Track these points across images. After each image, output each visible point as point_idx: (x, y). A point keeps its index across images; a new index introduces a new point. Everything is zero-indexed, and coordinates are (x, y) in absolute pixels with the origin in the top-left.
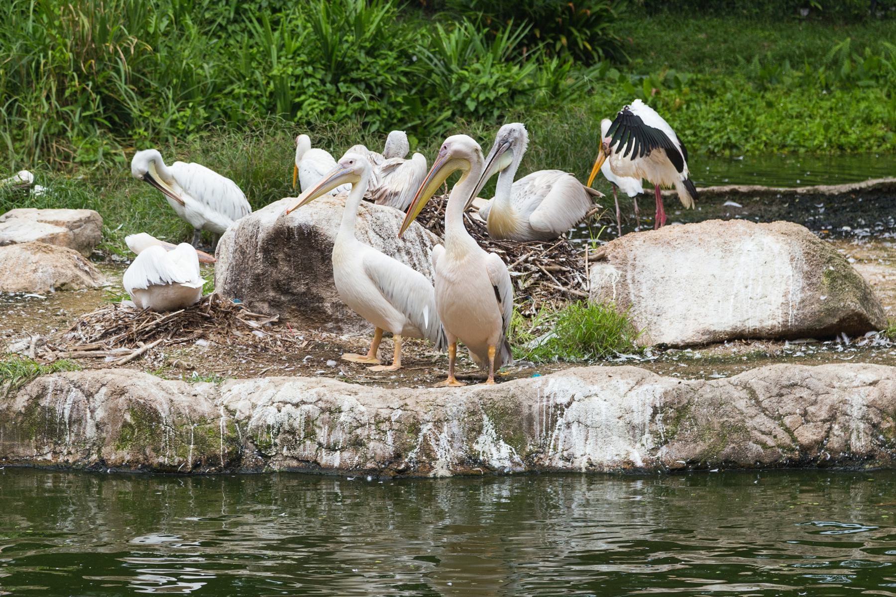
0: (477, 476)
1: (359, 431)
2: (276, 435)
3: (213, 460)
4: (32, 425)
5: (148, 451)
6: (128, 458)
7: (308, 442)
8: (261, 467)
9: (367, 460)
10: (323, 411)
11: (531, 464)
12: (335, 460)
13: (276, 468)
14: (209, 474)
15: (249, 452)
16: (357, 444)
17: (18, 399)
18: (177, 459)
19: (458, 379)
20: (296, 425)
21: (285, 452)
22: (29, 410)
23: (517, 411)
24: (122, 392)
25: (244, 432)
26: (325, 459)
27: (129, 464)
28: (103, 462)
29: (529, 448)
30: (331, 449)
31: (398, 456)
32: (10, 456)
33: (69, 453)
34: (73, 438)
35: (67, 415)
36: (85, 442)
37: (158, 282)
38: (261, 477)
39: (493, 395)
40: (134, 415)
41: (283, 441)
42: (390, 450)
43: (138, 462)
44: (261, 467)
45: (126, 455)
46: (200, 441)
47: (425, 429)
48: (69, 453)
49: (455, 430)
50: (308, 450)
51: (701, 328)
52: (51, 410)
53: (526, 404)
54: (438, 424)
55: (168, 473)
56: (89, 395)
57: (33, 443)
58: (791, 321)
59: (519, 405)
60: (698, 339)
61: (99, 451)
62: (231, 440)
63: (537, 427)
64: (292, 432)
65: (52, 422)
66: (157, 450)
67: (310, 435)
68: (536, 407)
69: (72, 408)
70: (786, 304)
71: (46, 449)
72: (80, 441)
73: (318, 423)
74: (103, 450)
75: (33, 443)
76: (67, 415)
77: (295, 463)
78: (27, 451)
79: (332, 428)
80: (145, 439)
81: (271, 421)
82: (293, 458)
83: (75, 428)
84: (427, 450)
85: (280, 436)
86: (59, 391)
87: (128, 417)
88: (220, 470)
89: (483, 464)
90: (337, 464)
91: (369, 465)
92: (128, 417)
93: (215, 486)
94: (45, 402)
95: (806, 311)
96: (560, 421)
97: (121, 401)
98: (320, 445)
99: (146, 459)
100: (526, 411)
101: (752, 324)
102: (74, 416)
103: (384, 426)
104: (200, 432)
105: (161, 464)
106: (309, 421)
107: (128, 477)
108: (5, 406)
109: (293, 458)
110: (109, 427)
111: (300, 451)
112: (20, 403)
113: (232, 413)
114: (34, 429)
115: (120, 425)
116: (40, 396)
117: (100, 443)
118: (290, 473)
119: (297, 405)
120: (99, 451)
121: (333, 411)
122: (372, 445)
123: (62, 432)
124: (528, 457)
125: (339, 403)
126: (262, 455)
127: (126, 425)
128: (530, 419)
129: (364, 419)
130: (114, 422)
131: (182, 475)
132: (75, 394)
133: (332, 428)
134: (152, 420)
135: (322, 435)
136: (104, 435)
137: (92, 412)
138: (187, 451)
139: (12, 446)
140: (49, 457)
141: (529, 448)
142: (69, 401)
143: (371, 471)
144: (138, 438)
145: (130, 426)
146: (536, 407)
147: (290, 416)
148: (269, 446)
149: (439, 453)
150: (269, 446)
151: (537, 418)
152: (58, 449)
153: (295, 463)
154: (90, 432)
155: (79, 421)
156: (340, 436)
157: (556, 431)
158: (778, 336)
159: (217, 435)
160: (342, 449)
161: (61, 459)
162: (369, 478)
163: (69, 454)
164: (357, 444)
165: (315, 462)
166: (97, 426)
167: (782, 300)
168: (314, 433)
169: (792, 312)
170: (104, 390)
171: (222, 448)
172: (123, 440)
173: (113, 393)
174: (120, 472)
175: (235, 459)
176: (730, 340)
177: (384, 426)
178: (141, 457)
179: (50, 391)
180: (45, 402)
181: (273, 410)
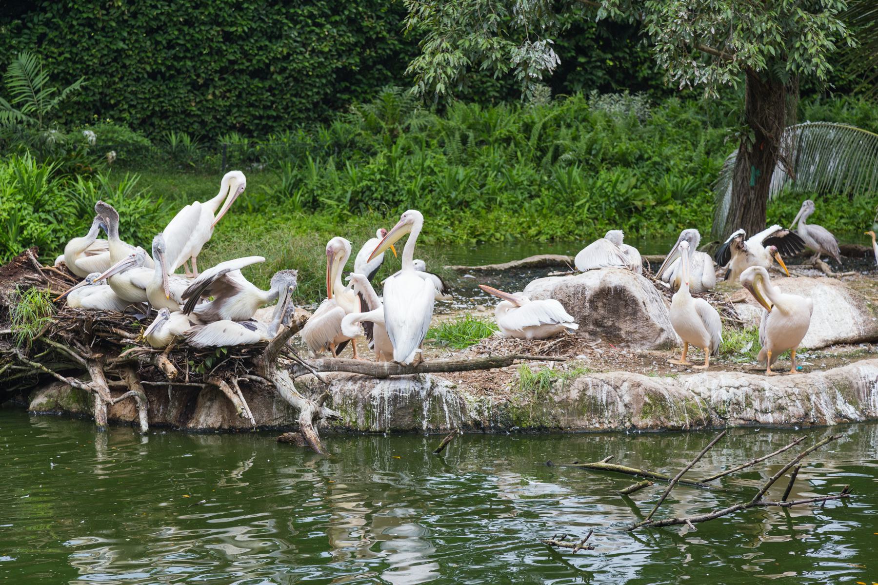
0: (845, 423)
1: (780, 401)
2: (728, 406)
3: (699, 422)
4: (583, 407)
5: (662, 418)
6: (650, 423)
7: (748, 409)
8: (724, 425)
9: (790, 417)
10: (754, 391)
11: (867, 417)
12: (770, 418)
13: (733, 425)
14: (699, 430)
15: (714, 416)
16: (781, 408)
17: (572, 392)
18: (681, 423)
19: (799, 371)
20: (740, 399)
21: (735, 415)
22: (581, 399)
23: (851, 387)
24: (639, 385)
25: (709, 405)
26: (762, 418)
27: (652, 427)
28: (634, 427)
29: (861, 407)
30: (765, 412)
31: (807, 415)
32: (572, 426)
33: (610, 422)
34: (610, 413)
35: (604, 400)
36: (619, 415)
37: (549, 321)
38: (724, 429)
39: (836, 378)
40: (650, 397)
41: (733, 409)
42: (802, 412)
43: (657, 425)
44: (724, 425)
45: (649, 421)
46: (690, 412)
47: (813, 398)
48: (610, 422)
49: (826, 398)
50: (749, 414)
51: (821, 338)
52: (594, 398)
53: (854, 381)
54: (817, 394)
55: (677, 431)
56: (616, 388)
57: (585, 418)
58: (863, 334)
59: (851, 383)
60: (822, 345)
61: (630, 420)
62: (705, 410)
63: (862, 395)
64: (738, 403)
65: (595, 404)
66: (668, 418)
67: (749, 405)
68: (860, 383)
69: (607, 396)
70: (856, 323)
71: (594, 421)
72: (615, 415)
73: (753, 397)
74: (632, 419)
75: (585, 418)
76: (604, 400)
77: (742, 422)
78: (582, 423)
79: (762, 400)
80: (659, 411)
81: (725, 398)
82: (741, 419)
83: (611, 407)
84: (818, 411)
85: (731, 406)
86: (596, 386)
87: (647, 399)
88: (705, 428)
89: (845, 417)
90: (771, 420)
91: (793, 420)
92: (647, 399)
93: (701, 437)
94: (590, 392)
95: (869, 326)
96: (873, 391)
97: (640, 389)
98: (756, 410)
99: (662, 423)
100: (856, 386)
101: (843, 336)
102: (610, 400)
103: (793, 397)
104: (689, 406)
105: (673, 426)
106: (747, 397)
107: (652, 435)
108: (565, 396)
109: (741, 419)
110: (635, 406)
111: (744, 415)
112: (574, 394)
113: (699, 394)
114: (585, 409)
115: (642, 404)
116: (584, 390)
117: (630, 416)
118: (742, 427)
119: (738, 388)
120: (630, 420)
121: (760, 390)
122: (790, 408)
123: (602, 410)
124: (862, 412)
125: (762, 386)
126: (723, 419)
127: (646, 404)
128: (858, 390)
129: (781, 394)
130: (638, 402)
131: (685, 431)
132: (606, 388)
133: (762, 400)
134: (662, 400)
135: (756, 404)
136: (631, 411)
137: (620, 397)
138: (685, 418)
139: (573, 420)
140: (597, 425)
141: (861, 407)
142: (604, 392)
143: (796, 424)
144: (655, 412)
145: (649, 404)
146: (860, 383)
147: (735, 394)
148: (725, 413)
149: (825, 412)
150: (725, 413)
151: (861, 390)
152: (601, 420)
153: (742, 422)
154: (621, 409)
155: (613, 403)
156: (769, 405)
157: (872, 397)
158: (855, 342)
159: (697, 408)
160: (772, 412)
161: (605, 426)
162: (797, 428)
163: (608, 422)
164: (781, 408)
165: (755, 420)
166: (626, 406)
167: (853, 321)
168: (751, 404)
169: (862, 328)
170: (626, 384)
171: (703, 415)
172: (645, 413)
173: (633, 385)
174: (646, 432)
175: (709, 420)
176: (833, 345)
177: (793, 397)
178: (659, 423)
179: (590, 385)
180: (590, 392)
181: (723, 391)
